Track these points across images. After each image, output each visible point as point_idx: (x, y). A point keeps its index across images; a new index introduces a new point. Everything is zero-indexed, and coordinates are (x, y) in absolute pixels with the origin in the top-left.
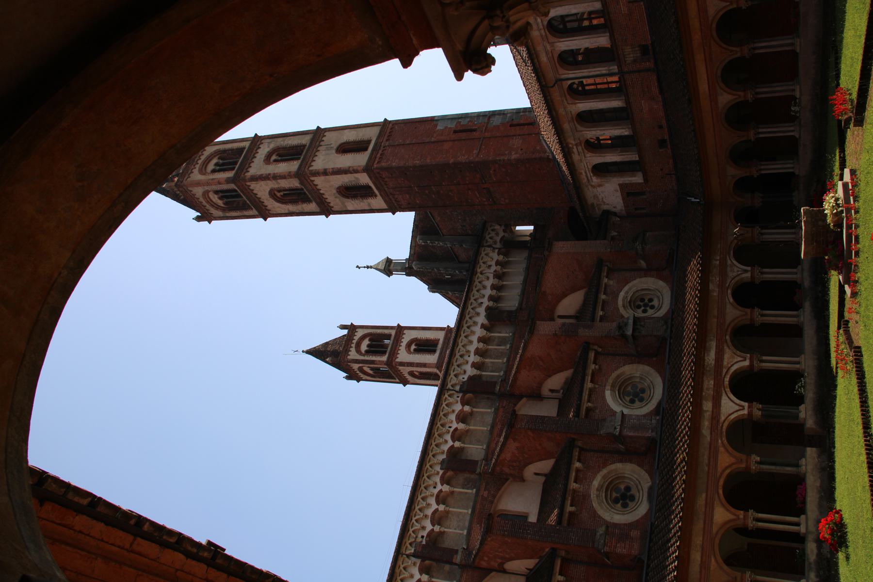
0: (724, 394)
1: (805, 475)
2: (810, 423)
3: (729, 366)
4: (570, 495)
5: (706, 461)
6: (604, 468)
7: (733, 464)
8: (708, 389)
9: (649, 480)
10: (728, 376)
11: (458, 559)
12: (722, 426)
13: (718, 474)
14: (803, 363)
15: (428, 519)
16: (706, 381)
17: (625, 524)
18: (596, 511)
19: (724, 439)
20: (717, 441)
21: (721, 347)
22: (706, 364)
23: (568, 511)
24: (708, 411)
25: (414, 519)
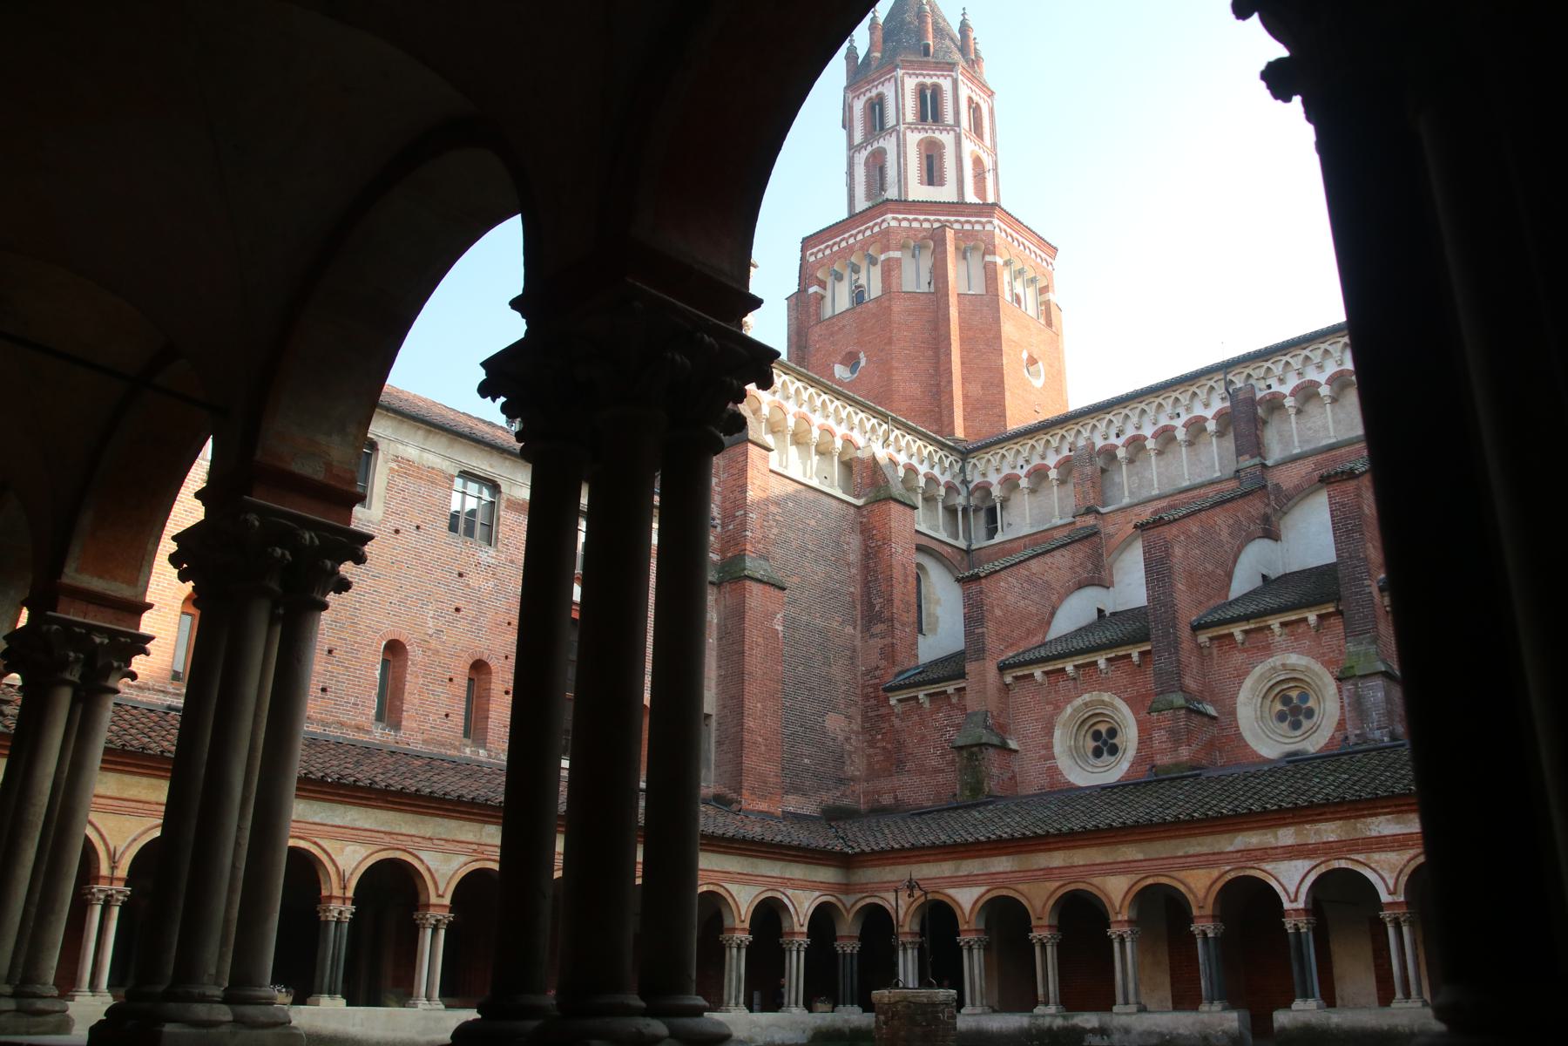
0: (1314, 863)
1: (1196, 1009)
2: (1281, 1018)
3: (1373, 865)
4: (1258, 625)
5: (1192, 851)
6: (1322, 664)
7: (1195, 896)
8: (1317, 832)
9: (1318, 747)
10: (1350, 865)
11: (1247, 462)
12: (1254, 868)
13: (1175, 874)
14: (1404, 1005)
15: (1299, 379)
16: (1333, 827)
17: (1238, 727)
18: (1248, 674)
19: (1233, 875)
20: (1228, 864)
21: (1410, 843)
22: (1369, 820)
23: (1232, 630)
24: (1277, 838)
25: (1287, 358)
